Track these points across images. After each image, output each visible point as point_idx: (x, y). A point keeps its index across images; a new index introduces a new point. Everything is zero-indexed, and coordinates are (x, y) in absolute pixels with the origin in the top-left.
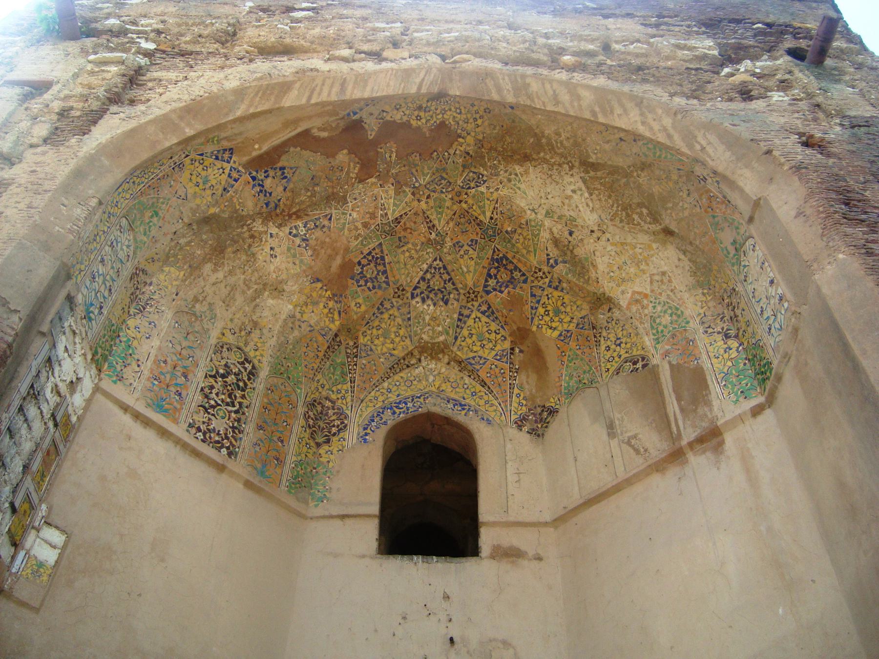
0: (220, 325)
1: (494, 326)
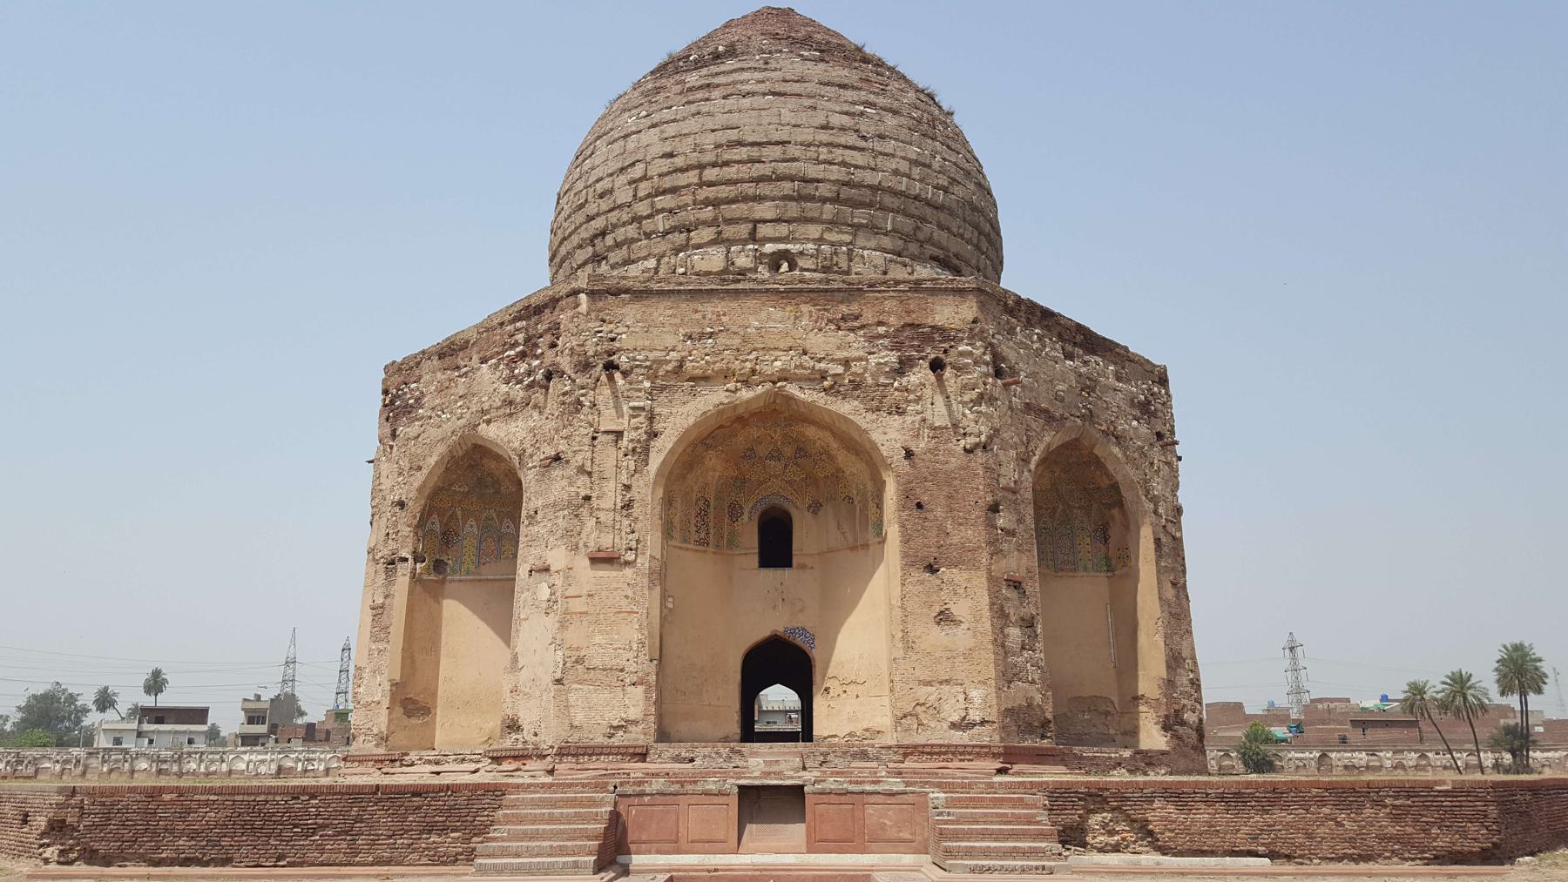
0: (695, 493)
1: (799, 469)
